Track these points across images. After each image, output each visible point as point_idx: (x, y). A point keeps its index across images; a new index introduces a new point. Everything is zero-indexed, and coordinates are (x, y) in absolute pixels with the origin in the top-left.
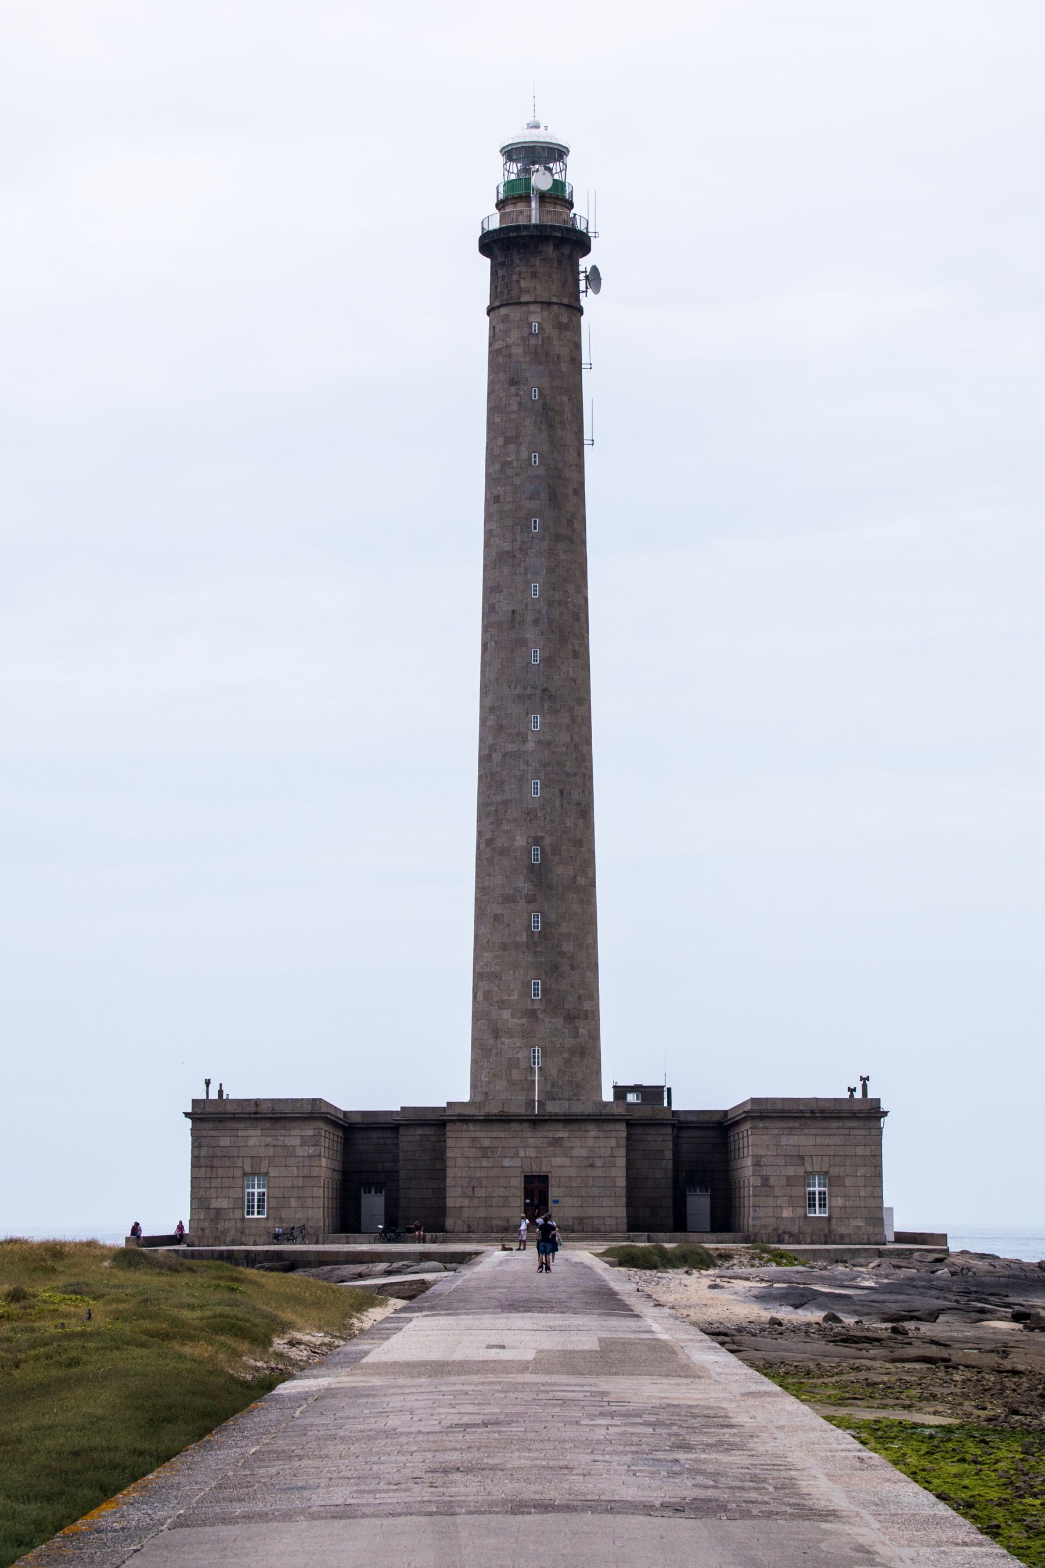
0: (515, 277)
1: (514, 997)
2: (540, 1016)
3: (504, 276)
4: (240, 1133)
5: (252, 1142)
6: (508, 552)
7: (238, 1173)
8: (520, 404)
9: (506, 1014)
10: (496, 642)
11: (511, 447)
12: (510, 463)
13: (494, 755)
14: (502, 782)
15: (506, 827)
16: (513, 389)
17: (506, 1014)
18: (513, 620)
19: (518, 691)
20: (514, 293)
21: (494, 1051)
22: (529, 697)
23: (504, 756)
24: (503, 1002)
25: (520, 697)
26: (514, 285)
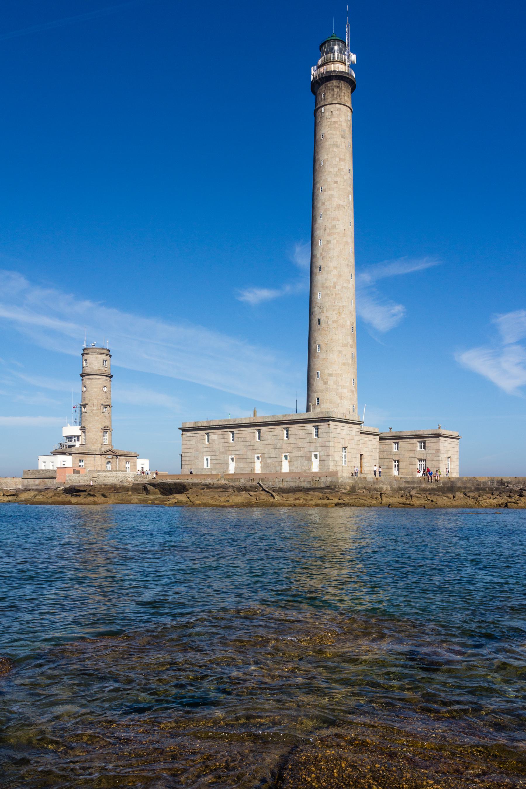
0: (343, 94)
1: (348, 384)
2: (355, 393)
3: (338, 92)
4: (342, 428)
5: (345, 432)
6: (342, 205)
7: (341, 446)
8: (345, 146)
9: (345, 391)
10: (337, 241)
11: (342, 163)
12: (342, 169)
13: (337, 287)
14: (341, 298)
15: (343, 316)
16: (343, 139)
17: (345, 391)
18: (344, 233)
19: (347, 263)
20: (343, 100)
21: (340, 405)
22: (350, 266)
23: (342, 287)
24: (343, 385)
25: (347, 265)
26: (343, 97)
